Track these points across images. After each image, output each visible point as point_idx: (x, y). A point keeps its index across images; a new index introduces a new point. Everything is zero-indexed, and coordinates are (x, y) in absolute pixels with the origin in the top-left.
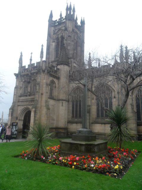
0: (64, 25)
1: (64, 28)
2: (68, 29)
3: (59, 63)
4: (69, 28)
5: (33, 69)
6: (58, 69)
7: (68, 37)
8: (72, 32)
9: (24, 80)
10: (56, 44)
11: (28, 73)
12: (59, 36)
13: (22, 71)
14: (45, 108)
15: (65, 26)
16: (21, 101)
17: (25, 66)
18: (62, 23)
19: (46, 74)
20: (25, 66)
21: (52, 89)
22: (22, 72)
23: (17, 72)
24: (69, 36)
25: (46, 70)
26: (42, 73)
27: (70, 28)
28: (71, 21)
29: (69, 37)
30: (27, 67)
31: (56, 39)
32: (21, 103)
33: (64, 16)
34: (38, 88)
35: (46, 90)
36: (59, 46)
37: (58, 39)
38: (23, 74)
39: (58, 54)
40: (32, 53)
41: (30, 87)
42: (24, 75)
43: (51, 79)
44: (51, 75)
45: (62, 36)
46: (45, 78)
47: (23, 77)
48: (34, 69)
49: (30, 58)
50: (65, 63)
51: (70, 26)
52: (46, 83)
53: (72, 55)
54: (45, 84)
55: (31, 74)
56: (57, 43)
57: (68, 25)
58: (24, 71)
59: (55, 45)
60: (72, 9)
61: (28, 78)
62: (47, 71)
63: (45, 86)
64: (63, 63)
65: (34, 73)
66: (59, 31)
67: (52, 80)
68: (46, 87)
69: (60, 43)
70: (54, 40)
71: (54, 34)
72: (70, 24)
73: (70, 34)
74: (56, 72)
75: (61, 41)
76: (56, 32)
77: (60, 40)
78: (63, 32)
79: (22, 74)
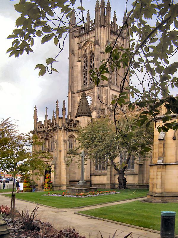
0: (94, 35)
1: (93, 40)
2: (100, 42)
3: (78, 115)
4: (102, 40)
5: (49, 125)
6: (78, 121)
7: (99, 54)
9: (41, 137)
10: (83, 64)
11: (44, 129)
12: (88, 52)
13: (38, 127)
15: (94, 36)
17: (41, 122)
18: (91, 31)
19: (63, 131)
20: (41, 122)
21: (72, 144)
22: (39, 128)
23: (33, 129)
25: (63, 128)
26: (59, 131)
27: (103, 39)
28: (104, 27)
29: (102, 54)
30: (43, 123)
31: (82, 57)
33: (93, 18)
34: (56, 146)
35: (64, 147)
36: (88, 68)
37: (85, 56)
38: (40, 130)
39: (87, 79)
41: (48, 144)
42: (41, 132)
43: (69, 134)
44: (69, 130)
45: (91, 52)
47: (40, 133)
48: (50, 126)
50: (85, 114)
51: (102, 37)
52: (64, 141)
54: (63, 141)
55: (48, 131)
56: (85, 62)
57: (99, 35)
58: (40, 127)
59: (82, 66)
60: (106, 7)
61: (45, 135)
62: (64, 128)
63: (62, 143)
64: (83, 114)
65: (51, 130)
66: (86, 43)
67: (71, 135)
68: (64, 144)
69: (88, 62)
70: (79, 58)
71: (79, 49)
72: (102, 33)
74: (75, 125)
75: (91, 60)
76: (81, 46)
77: (89, 58)
78: (92, 46)
79: (38, 130)
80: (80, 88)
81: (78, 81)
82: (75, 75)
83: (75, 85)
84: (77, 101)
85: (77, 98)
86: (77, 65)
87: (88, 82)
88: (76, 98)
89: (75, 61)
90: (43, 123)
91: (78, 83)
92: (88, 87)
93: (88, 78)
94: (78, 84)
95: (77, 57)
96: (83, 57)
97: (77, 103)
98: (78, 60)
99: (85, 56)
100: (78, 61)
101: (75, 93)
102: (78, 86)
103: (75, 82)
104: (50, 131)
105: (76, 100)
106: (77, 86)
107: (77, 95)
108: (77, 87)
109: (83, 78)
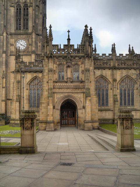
8: (40, 2)
9: (58, 63)
14: (95, 97)
16: (57, 87)
24: (37, 6)
32: (58, 89)
40: (69, 32)
46: (91, 64)
49: (67, 38)
53: (41, 31)
56: (17, 9)
73: (38, 4)
80: (13, 31)
81: (10, 24)
82: (9, 18)
83: (9, 27)
84: (10, 42)
85: (10, 40)
86: (10, 10)
87: (22, 28)
88: (9, 40)
89: (9, 5)
90: (76, 47)
91: (10, 26)
92: (22, 32)
93: (22, 24)
94: (11, 27)
95: (10, 2)
96: (15, 4)
97: (10, 44)
98: (11, 5)
99: (18, 4)
100: (11, 6)
101: (8, 34)
102: (11, 29)
103: (8, 24)
104: (74, 58)
105: (9, 41)
106: (10, 28)
107: (10, 37)
108: (10, 29)
109: (15, 23)
